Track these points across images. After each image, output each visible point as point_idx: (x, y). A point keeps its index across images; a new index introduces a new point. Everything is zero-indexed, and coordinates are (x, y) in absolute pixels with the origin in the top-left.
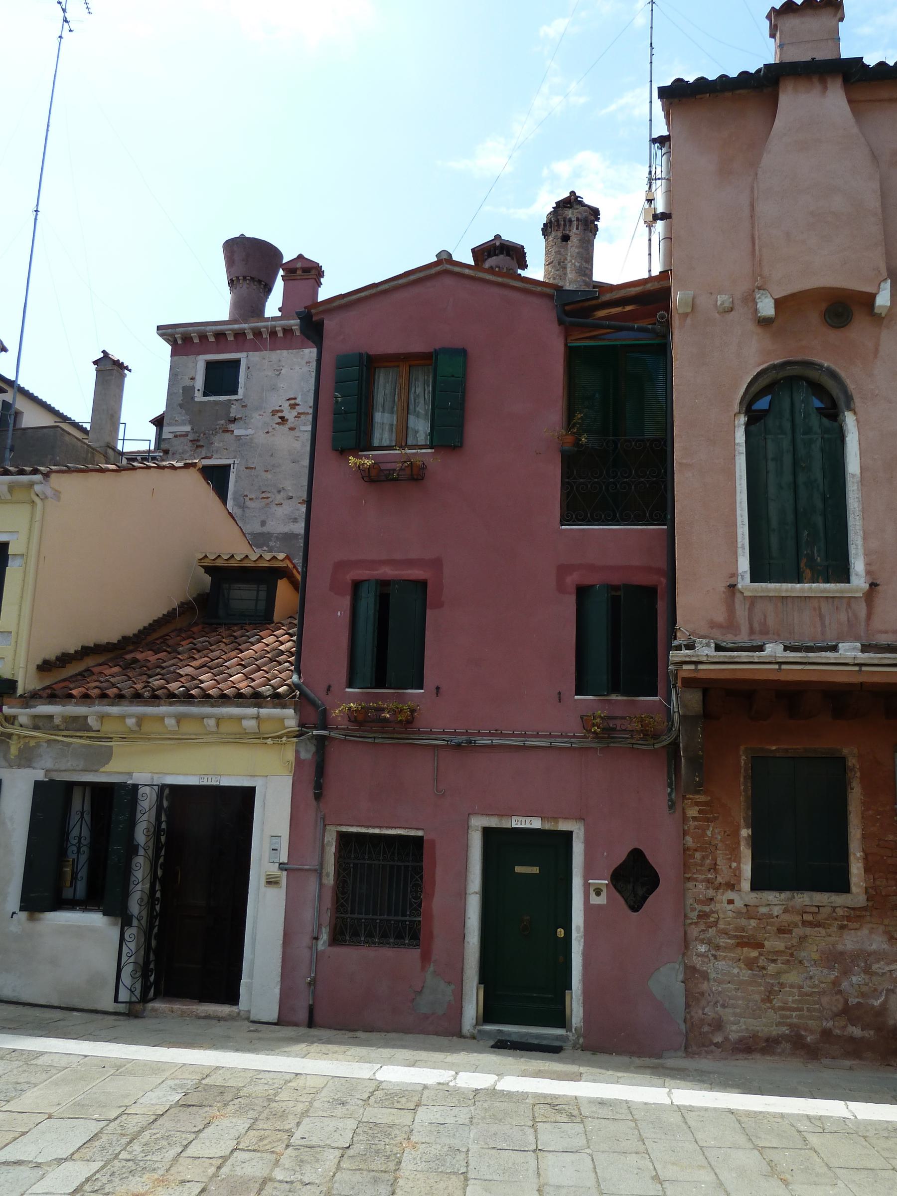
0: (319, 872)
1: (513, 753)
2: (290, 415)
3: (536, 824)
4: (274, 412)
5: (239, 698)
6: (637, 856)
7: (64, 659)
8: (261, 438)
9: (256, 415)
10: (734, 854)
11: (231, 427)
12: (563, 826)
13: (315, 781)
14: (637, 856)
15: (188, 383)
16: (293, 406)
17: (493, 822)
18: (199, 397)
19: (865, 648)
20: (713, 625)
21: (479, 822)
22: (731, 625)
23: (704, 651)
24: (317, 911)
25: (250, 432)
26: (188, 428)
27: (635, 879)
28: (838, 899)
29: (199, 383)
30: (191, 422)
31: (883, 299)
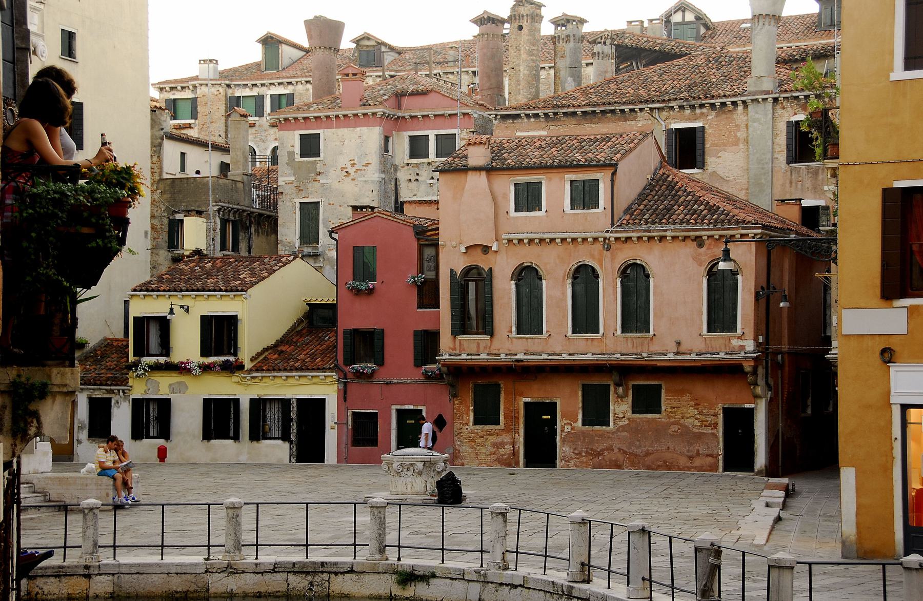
0: (347, 424)
1: (400, 385)
2: (352, 171)
3: (411, 407)
4: (342, 169)
5: (318, 369)
6: (440, 416)
7: (259, 355)
8: (336, 185)
9: (332, 171)
10: (468, 415)
11: (318, 178)
12: (419, 408)
13: (344, 396)
14: (440, 416)
15: (291, 149)
16: (353, 165)
17: (399, 407)
18: (298, 158)
19: (488, 355)
20: (450, 348)
21: (394, 407)
22: (454, 349)
23: (446, 357)
24: (347, 438)
25: (329, 181)
26: (293, 178)
27: (440, 423)
28: (498, 427)
29: (297, 150)
30: (294, 175)
31: (494, 248)
